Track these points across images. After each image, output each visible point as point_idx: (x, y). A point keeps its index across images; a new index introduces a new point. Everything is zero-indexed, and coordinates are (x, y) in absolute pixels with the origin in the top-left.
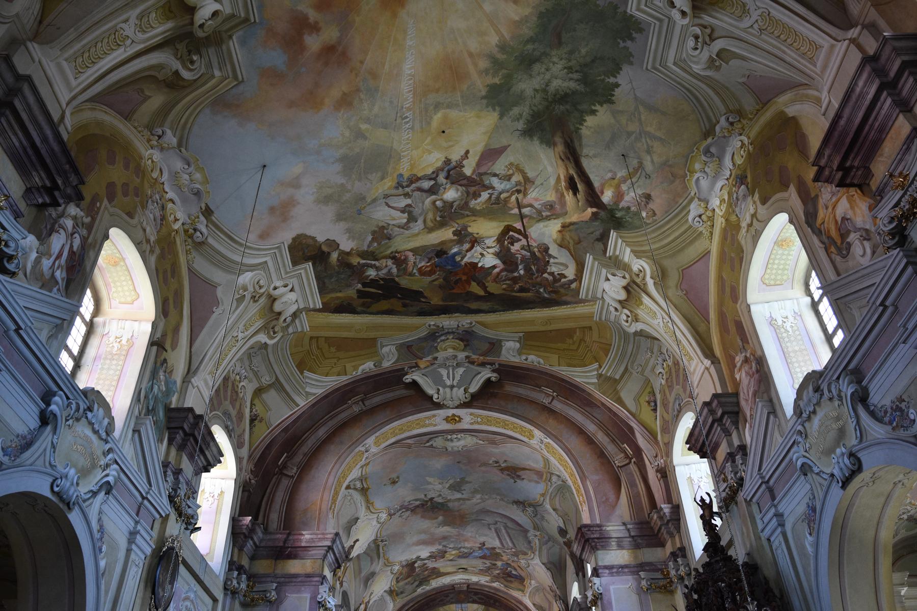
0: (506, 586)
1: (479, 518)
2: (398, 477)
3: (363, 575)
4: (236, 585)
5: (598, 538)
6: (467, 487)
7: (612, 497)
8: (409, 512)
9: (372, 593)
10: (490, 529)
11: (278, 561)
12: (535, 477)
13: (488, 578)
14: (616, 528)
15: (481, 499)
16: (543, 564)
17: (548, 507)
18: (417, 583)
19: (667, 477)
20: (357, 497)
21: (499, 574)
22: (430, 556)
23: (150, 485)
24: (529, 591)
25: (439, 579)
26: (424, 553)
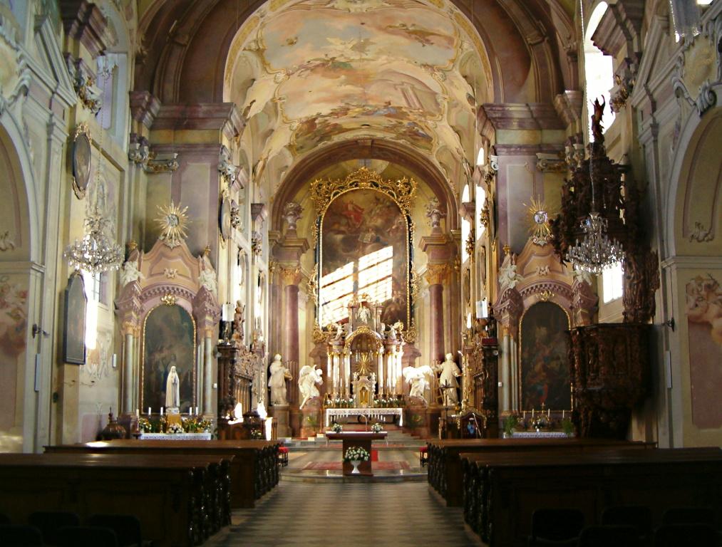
0: (412, 144)
1: (385, 78)
2: (296, 38)
4: (140, 156)
5: (499, 118)
6: (371, 47)
7: (519, 76)
8: (309, 71)
9: (270, 150)
10: (396, 89)
11: (177, 132)
12: (445, 42)
13: (394, 135)
14: (519, 109)
15: (387, 59)
16: (452, 127)
17: (457, 73)
18: (317, 139)
19: (576, 61)
20: (253, 58)
21: (405, 132)
22: (332, 113)
23: (57, 80)
25: (341, 135)
26: (325, 109)
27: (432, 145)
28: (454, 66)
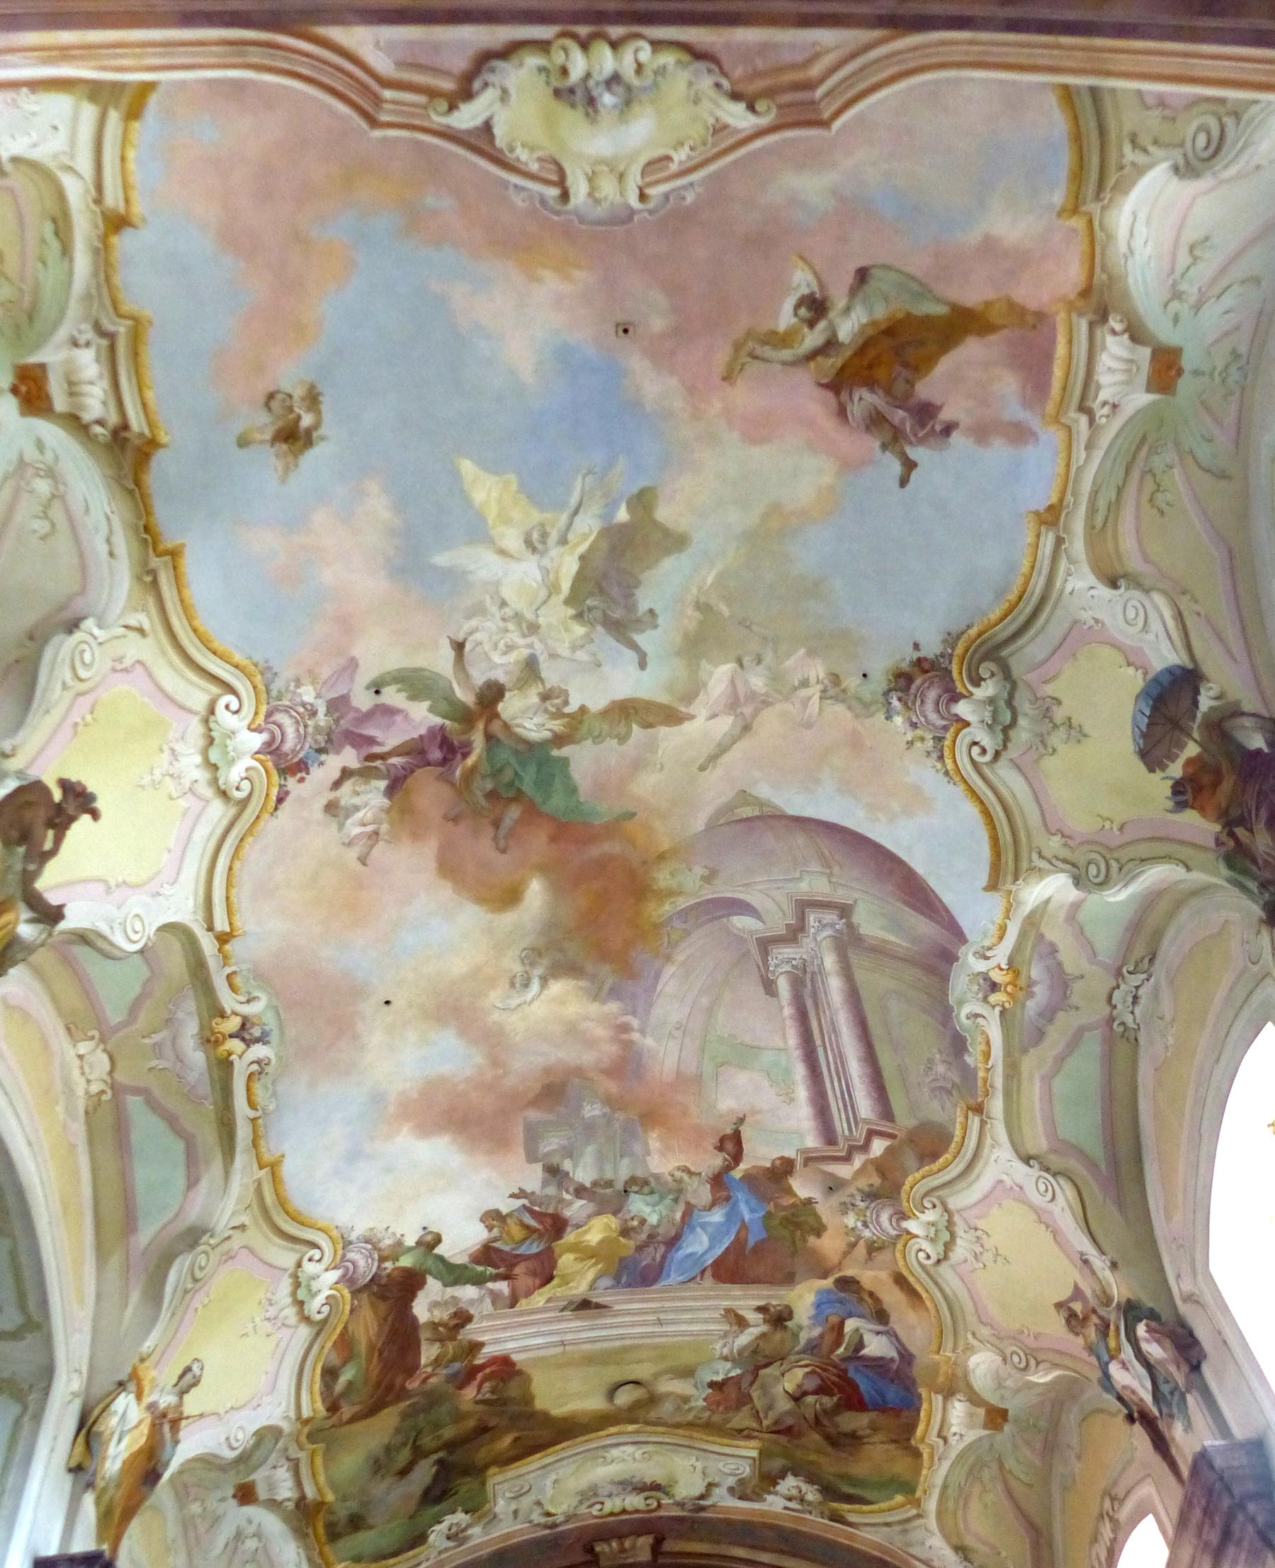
3: (145, 1235)
24: (939, 1481)
27: (917, 1454)
28: (1059, 541)
